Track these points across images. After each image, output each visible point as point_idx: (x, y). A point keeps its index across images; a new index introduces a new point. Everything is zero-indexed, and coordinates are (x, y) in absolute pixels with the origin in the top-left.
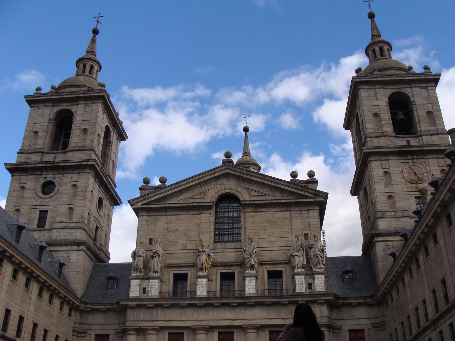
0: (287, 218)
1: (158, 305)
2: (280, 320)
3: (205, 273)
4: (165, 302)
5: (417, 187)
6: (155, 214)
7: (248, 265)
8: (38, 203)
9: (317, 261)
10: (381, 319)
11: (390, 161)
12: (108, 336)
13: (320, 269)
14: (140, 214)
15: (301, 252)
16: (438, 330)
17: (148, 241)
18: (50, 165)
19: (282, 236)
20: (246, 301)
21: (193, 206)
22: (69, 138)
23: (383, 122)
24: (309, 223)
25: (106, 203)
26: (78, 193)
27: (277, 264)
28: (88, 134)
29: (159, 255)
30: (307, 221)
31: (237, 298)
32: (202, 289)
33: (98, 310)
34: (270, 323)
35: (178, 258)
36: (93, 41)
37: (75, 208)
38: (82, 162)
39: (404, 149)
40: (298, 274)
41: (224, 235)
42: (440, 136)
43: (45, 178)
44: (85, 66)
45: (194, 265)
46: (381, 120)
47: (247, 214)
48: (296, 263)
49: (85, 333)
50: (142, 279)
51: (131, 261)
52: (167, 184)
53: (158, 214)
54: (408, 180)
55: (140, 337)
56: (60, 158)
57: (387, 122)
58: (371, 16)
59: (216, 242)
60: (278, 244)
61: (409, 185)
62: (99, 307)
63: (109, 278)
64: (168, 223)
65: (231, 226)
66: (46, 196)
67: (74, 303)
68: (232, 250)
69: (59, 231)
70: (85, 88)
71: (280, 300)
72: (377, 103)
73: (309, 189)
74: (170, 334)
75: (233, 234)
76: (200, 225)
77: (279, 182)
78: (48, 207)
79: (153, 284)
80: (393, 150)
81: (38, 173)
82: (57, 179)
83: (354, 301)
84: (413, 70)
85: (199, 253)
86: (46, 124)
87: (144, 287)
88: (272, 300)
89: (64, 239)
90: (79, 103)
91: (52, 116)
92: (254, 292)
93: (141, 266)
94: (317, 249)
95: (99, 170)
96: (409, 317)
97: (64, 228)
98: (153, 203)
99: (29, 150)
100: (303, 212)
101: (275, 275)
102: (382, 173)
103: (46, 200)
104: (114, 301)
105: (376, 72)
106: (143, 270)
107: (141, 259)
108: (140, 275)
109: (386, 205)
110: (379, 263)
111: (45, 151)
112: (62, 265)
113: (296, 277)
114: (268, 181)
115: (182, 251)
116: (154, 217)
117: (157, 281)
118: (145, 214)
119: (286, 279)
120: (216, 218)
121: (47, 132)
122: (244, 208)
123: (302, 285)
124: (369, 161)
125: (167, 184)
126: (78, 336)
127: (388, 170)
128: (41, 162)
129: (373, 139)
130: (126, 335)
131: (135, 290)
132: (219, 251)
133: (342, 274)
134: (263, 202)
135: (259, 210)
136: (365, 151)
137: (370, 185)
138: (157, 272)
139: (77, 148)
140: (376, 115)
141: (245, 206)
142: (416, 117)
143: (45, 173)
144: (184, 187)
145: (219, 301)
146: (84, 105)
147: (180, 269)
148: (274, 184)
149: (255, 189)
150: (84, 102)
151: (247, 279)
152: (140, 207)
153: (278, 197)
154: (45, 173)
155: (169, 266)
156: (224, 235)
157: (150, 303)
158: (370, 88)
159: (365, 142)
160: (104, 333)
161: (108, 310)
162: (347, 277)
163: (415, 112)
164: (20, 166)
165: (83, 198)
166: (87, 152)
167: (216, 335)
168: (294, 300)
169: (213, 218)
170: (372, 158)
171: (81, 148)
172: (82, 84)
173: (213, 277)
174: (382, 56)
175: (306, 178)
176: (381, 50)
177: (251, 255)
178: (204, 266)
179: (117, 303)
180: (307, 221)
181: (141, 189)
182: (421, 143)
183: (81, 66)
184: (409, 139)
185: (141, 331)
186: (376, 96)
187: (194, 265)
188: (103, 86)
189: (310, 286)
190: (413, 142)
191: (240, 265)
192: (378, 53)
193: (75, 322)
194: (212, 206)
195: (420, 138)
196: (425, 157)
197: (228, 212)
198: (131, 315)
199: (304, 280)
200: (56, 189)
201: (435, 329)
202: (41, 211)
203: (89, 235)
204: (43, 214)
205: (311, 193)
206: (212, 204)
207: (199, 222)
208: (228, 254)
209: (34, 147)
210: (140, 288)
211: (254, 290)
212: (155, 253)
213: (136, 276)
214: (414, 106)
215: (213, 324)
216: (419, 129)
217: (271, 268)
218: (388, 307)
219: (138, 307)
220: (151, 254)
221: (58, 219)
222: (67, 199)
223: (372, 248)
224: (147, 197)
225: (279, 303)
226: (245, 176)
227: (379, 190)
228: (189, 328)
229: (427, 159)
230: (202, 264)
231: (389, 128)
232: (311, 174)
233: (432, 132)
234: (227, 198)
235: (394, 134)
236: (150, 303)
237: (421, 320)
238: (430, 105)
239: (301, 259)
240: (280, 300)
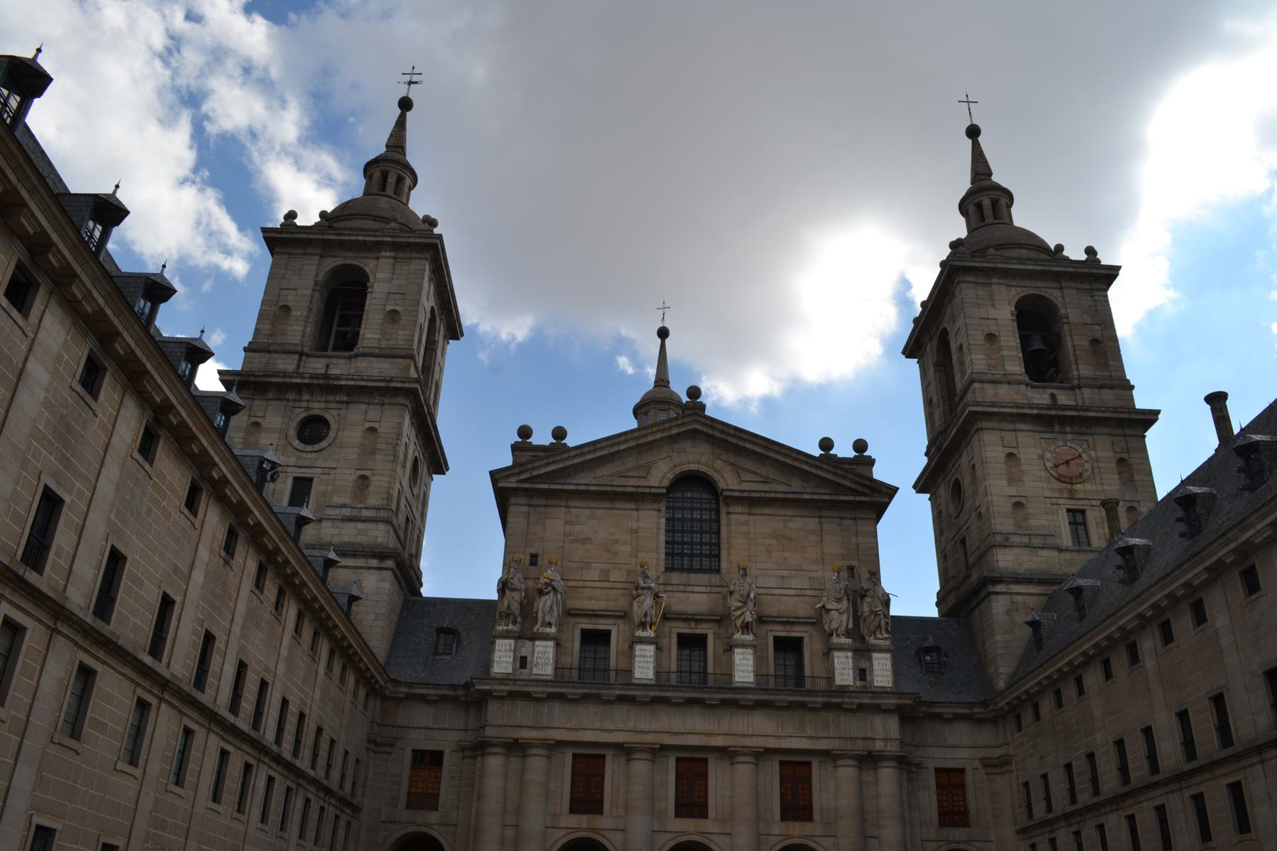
0: (813, 532)
1: (554, 694)
2: (804, 740)
3: (650, 633)
4: (571, 690)
5: (1071, 491)
6: (543, 502)
7: (739, 623)
8: (292, 461)
9: (876, 623)
10: (999, 752)
11: (1019, 434)
12: (441, 753)
13: (882, 639)
14: (512, 500)
15: (845, 602)
16: (1188, 793)
17: (528, 558)
18: (321, 382)
20: (738, 696)
21: (623, 493)
22: (360, 326)
23: (1005, 353)
24: (857, 545)
25: (423, 469)
26: (379, 446)
27: (793, 623)
28: (402, 323)
29: (554, 589)
30: (854, 540)
31: (719, 689)
32: (644, 666)
33: (422, 699)
34: (784, 746)
35: (591, 598)
36: (401, 124)
37: (374, 479)
38: (391, 380)
39: (1049, 412)
40: (840, 648)
41: (682, 555)
42: (1116, 391)
43: (307, 409)
44: (385, 176)
45: (624, 616)
46: (1001, 349)
47: (733, 517)
48: (834, 626)
49: (392, 745)
50: (519, 637)
51: (494, 596)
52: (571, 441)
53: (550, 502)
55: (512, 759)
56: (340, 367)
57: (1013, 353)
58: (973, 132)
59: (668, 569)
60: (795, 583)
61: (1056, 484)
62: (424, 691)
63: (441, 630)
64: (568, 523)
65: (696, 538)
66: (309, 448)
67: (377, 682)
68: (702, 589)
69: (338, 524)
70: (393, 225)
71: (806, 699)
72: (993, 314)
73: (860, 476)
74: (575, 756)
75: (701, 555)
76: (636, 531)
77: (801, 457)
78: (314, 470)
79: (542, 649)
80: (1027, 411)
81: (291, 396)
82: (334, 412)
83: (947, 710)
84: (1065, 253)
85: (635, 591)
86: (309, 292)
87: (524, 654)
88: (791, 699)
89: (353, 544)
90: (383, 254)
91: (321, 278)
92: (752, 680)
93: (516, 607)
96: (1091, 756)
98: (536, 481)
99: (269, 344)
100: (845, 522)
101: (789, 647)
102: (1003, 455)
103: (309, 456)
104: (460, 679)
105: (992, 251)
106: (519, 620)
107: (517, 596)
108: (516, 628)
109: (1011, 521)
110: (999, 638)
111: (306, 350)
112: (353, 599)
113: (836, 654)
114: (778, 453)
115: (599, 584)
116: (543, 509)
117: (551, 643)
118: (523, 501)
119: (812, 655)
120: (667, 519)
121: (310, 310)
122: (727, 505)
123: (846, 672)
124: (978, 430)
125: (571, 441)
126: (375, 752)
127: (1014, 451)
128: (297, 373)
129: (986, 386)
130: (482, 755)
132: (675, 588)
133: (917, 652)
134: (768, 495)
135: (757, 511)
136: (972, 409)
137: (974, 477)
138: (550, 624)
140: (991, 337)
141: (730, 500)
142: (1070, 348)
143: (306, 397)
144: (606, 452)
145: (682, 694)
146: (391, 261)
147: (594, 620)
148: (789, 461)
149: (749, 467)
150: (393, 254)
151: (737, 650)
152: (514, 485)
153: (796, 486)
154: (306, 397)
155: (570, 613)
156: (682, 555)
157: (540, 689)
158: (980, 281)
159: (966, 390)
160: (431, 748)
161: (443, 699)
162: (928, 658)
163: (1068, 338)
164: (252, 379)
165: (391, 458)
167: (672, 763)
168: (834, 700)
169: (663, 520)
170: (984, 424)
171: (386, 352)
172: (389, 215)
173: (664, 642)
175: (851, 454)
176: (995, 204)
177: (745, 603)
178: (649, 619)
179: (467, 686)
180: (854, 540)
181: (515, 448)
182: (1080, 402)
183: (377, 174)
184: (1055, 391)
185: (516, 748)
186: (992, 300)
187: (624, 616)
188: (432, 223)
189: (862, 674)
190: (1063, 399)
191: (718, 621)
192: (988, 211)
193: (372, 722)
194: (662, 494)
195: (1077, 391)
196: (1088, 431)
197: (692, 509)
198: (495, 712)
199: (850, 661)
200: (332, 434)
201: (1181, 789)
202: (296, 479)
205: (864, 486)
207: (635, 526)
208: (695, 596)
209: (281, 339)
210: (514, 658)
212: (548, 585)
213: (508, 631)
214: (1066, 327)
215: (668, 740)
216: (1075, 373)
217: (781, 632)
218: (1020, 729)
219: (513, 696)
220: (540, 586)
221: (336, 500)
222: (355, 456)
223: (978, 605)
224: (530, 466)
225: (803, 706)
226: (730, 439)
227: (997, 490)
228: (619, 747)
229: (1091, 434)
230: (646, 615)
231: (1016, 367)
232: (860, 446)
234: (691, 480)
235: (1027, 379)
236: (540, 689)
237: (1131, 766)
238: (1098, 327)
239: (844, 617)
240: (806, 699)
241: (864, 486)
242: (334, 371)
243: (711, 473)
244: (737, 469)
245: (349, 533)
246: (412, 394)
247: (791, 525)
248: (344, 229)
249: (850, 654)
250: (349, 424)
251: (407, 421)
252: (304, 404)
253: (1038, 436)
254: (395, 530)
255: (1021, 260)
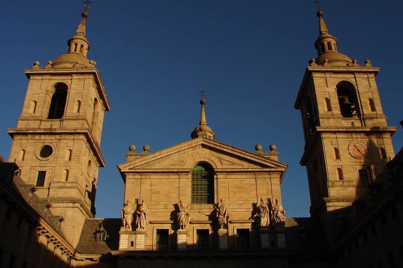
0: (253, 185)
3: (184, 230)
8: (37, 165)
19: (249, 199)
35: (160, 216)
40: (264, 232)
44: (76, 45)
54: (353, 156)
66: (44, 159)
69: (56, 190)
72: (327, 90)
79: (140, 238)
86: (44, 95)
92: (227, 247)
94: (279, 212)
95: (91, 138)
97: (61, 187)
111: (43, 119)
112: (61, 220)
113: (262, 235)
117: (143, 236)
122: (216, 175)
127: (337, 147)
131: (124, 244)
132: (195, 211)
139: (71, 118)
142: (359, 103)
148: (242, 156)
152: (128, 171)
153: (246, 165)
163: (358, 99)
165: (78, 162)
166: (80, 121)
169: (190, 183)
174: (329, 49)
184: (353, 121)
189: (273, 243)
199: (268, 238)
200: (53, 152)
202: (39, 172)
203: (81, 194)
204: (42, 175)
205: (274, 164)
206: (190, 170)
211: (227, 245)
213: (125, 231)
224: (134, 163)
230: (182, 222)
233: (372, 116)
235: (341, 116)
241: (274, 164)
242: (54, 127)
243: (210, 162)
244: (220, 160)
245: (61, 193)
246: (86, 134)
247: (243, 182)
248: (58, 68)
249: (268, 235)
250: (62, 148)
251: (84, 146)
252: (42, 141)
253: (346, 140)
254: (80, 191)
255: (338, 67)
